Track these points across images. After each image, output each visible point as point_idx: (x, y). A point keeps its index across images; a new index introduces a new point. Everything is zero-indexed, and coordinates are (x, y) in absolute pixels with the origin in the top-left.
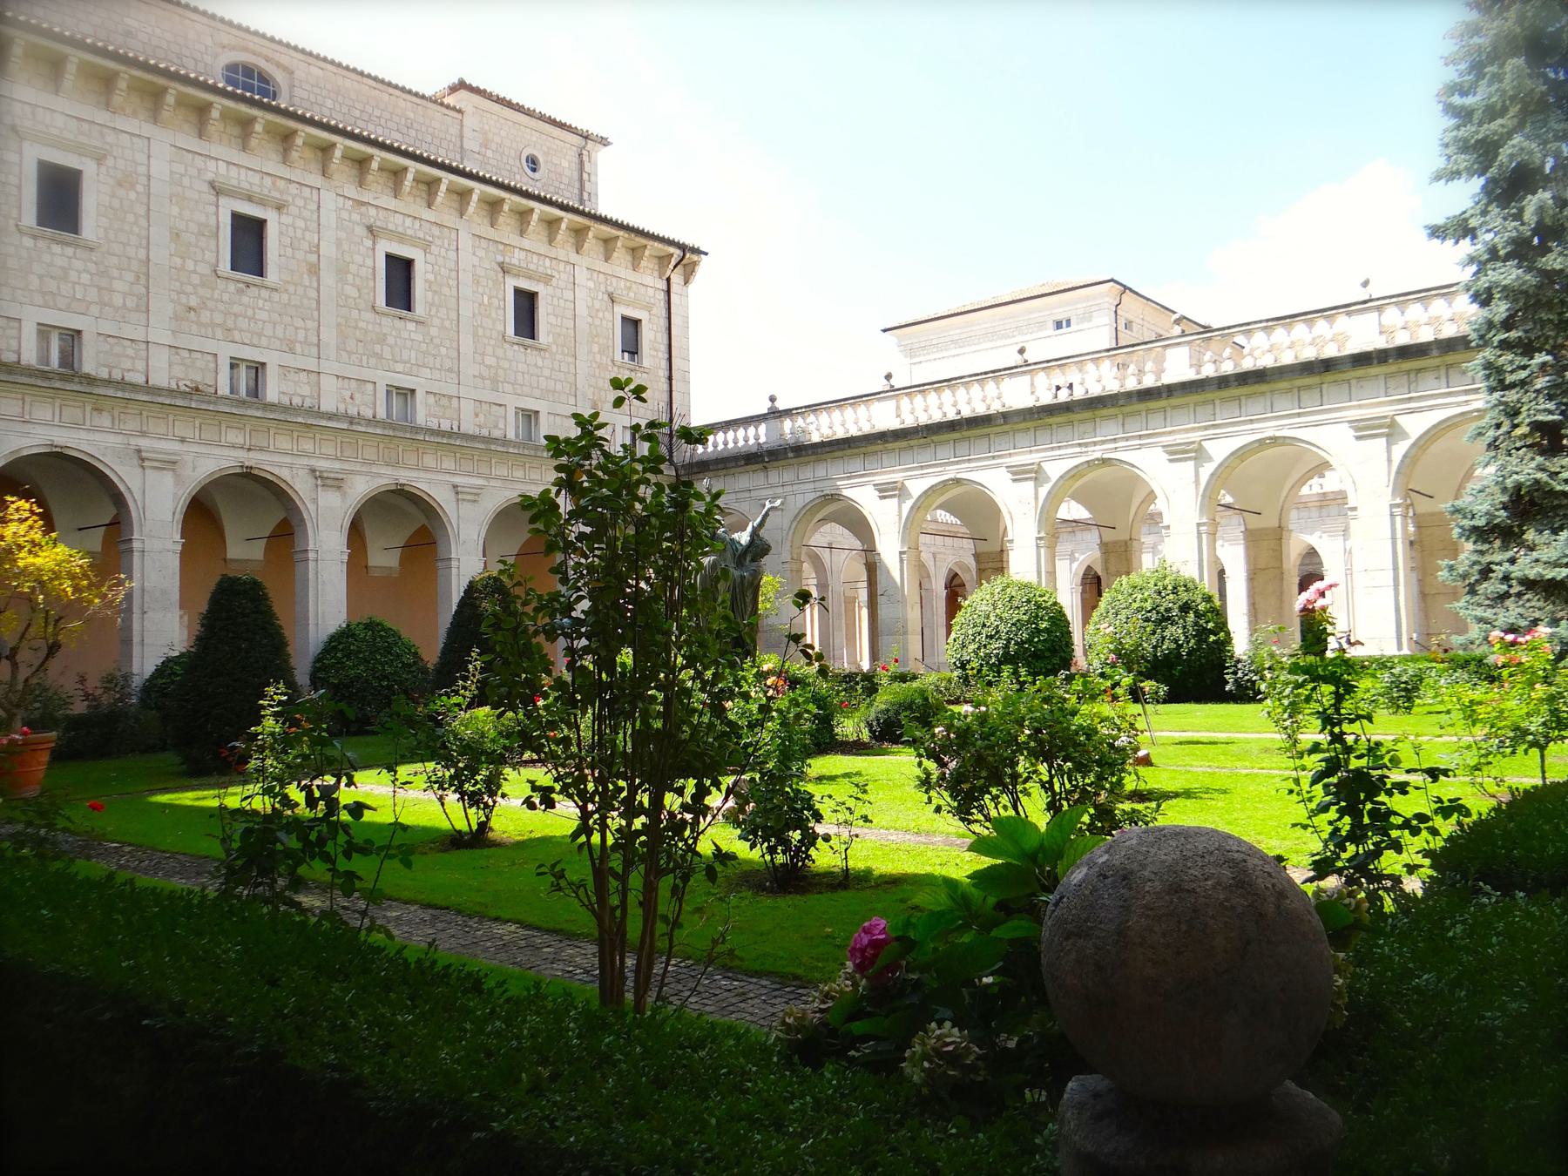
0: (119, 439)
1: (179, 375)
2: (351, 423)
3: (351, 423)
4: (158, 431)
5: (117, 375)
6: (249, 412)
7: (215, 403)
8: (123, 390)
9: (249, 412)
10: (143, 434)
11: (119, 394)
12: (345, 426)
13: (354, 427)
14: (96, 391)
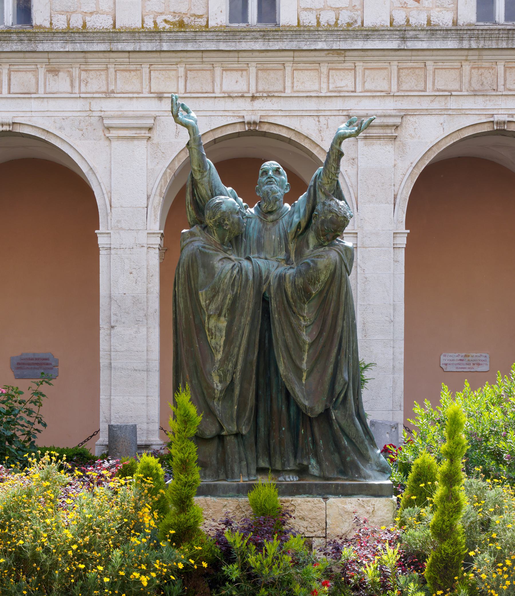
0: (79, 105)
1: (157, 9)
2: (404, 39)
3: (404, 39)
4: (129, 88)
5: (76, 22)
6: (244, 45)
7: (194, 40)
8: (73, 41)
9: (244, 45)
10: (109, 95)
11: (69, 47)
12: (394, 45)
13: (410, 45)
14: (40, 47)
